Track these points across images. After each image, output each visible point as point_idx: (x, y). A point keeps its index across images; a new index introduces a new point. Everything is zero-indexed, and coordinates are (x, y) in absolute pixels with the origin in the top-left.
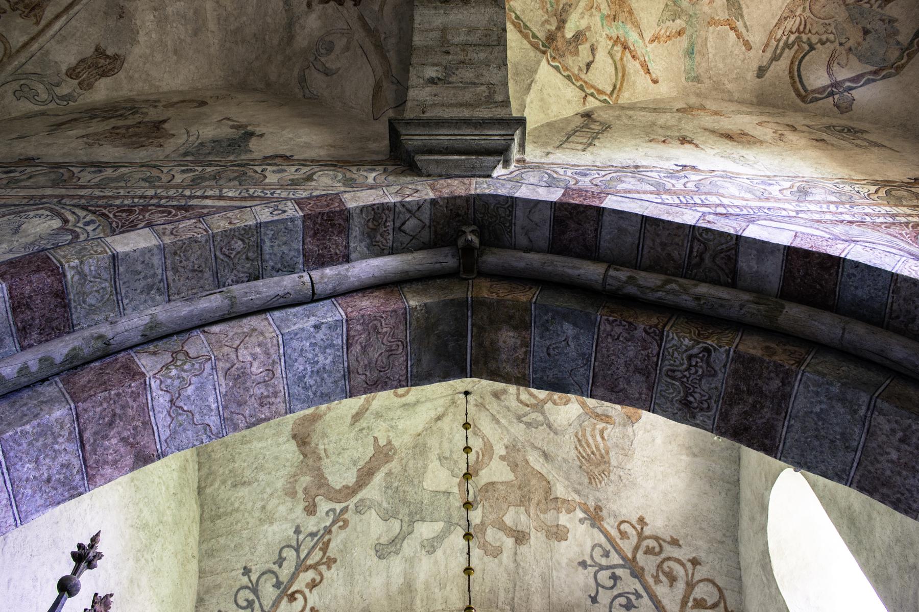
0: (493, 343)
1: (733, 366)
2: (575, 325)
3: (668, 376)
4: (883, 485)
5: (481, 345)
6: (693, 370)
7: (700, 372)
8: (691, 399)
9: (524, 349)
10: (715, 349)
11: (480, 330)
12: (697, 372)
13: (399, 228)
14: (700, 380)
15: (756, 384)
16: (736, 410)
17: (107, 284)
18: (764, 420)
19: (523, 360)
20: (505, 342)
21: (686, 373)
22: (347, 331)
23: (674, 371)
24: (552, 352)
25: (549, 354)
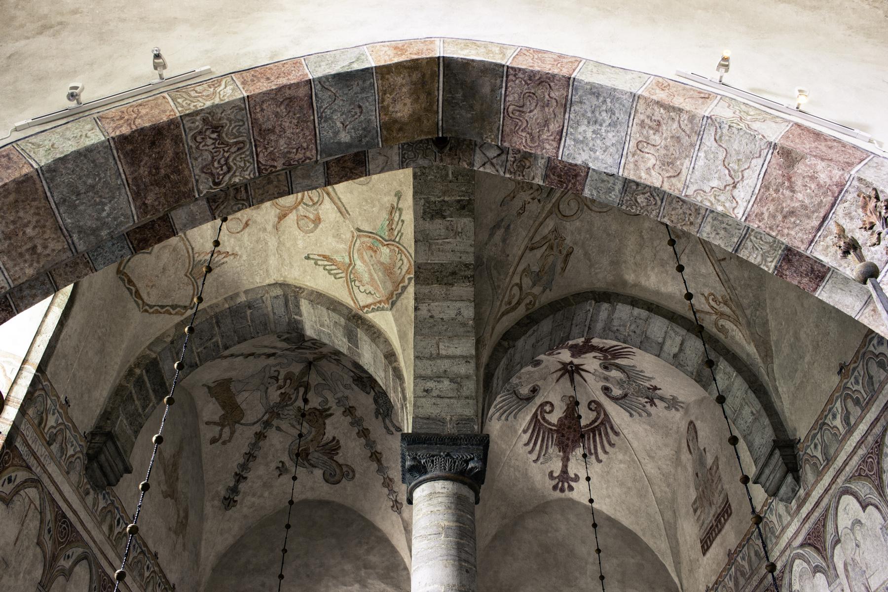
0: (417, 100)
1: (190, 186)
2: (339, 143)
3: (243, 142)
4: (16, 201)
5: (429, 94)
6: (223, 162)
7: (216, 164)
8: (214, 136)
9: (385, 103)
10: (211, 188)
11: (430, 109)
12: (219, 162)
13: (502, 152)
14: (213, 158)
15: (165, 186)
16: (170, 153)
17: (752, 237)
18: (142, 163)
19: (385, 93)
20: (405, 104)
21: (226, 155)
22: (559, 148)
23: (239, 149)
24: (358, 110)
25: (360, 107)
